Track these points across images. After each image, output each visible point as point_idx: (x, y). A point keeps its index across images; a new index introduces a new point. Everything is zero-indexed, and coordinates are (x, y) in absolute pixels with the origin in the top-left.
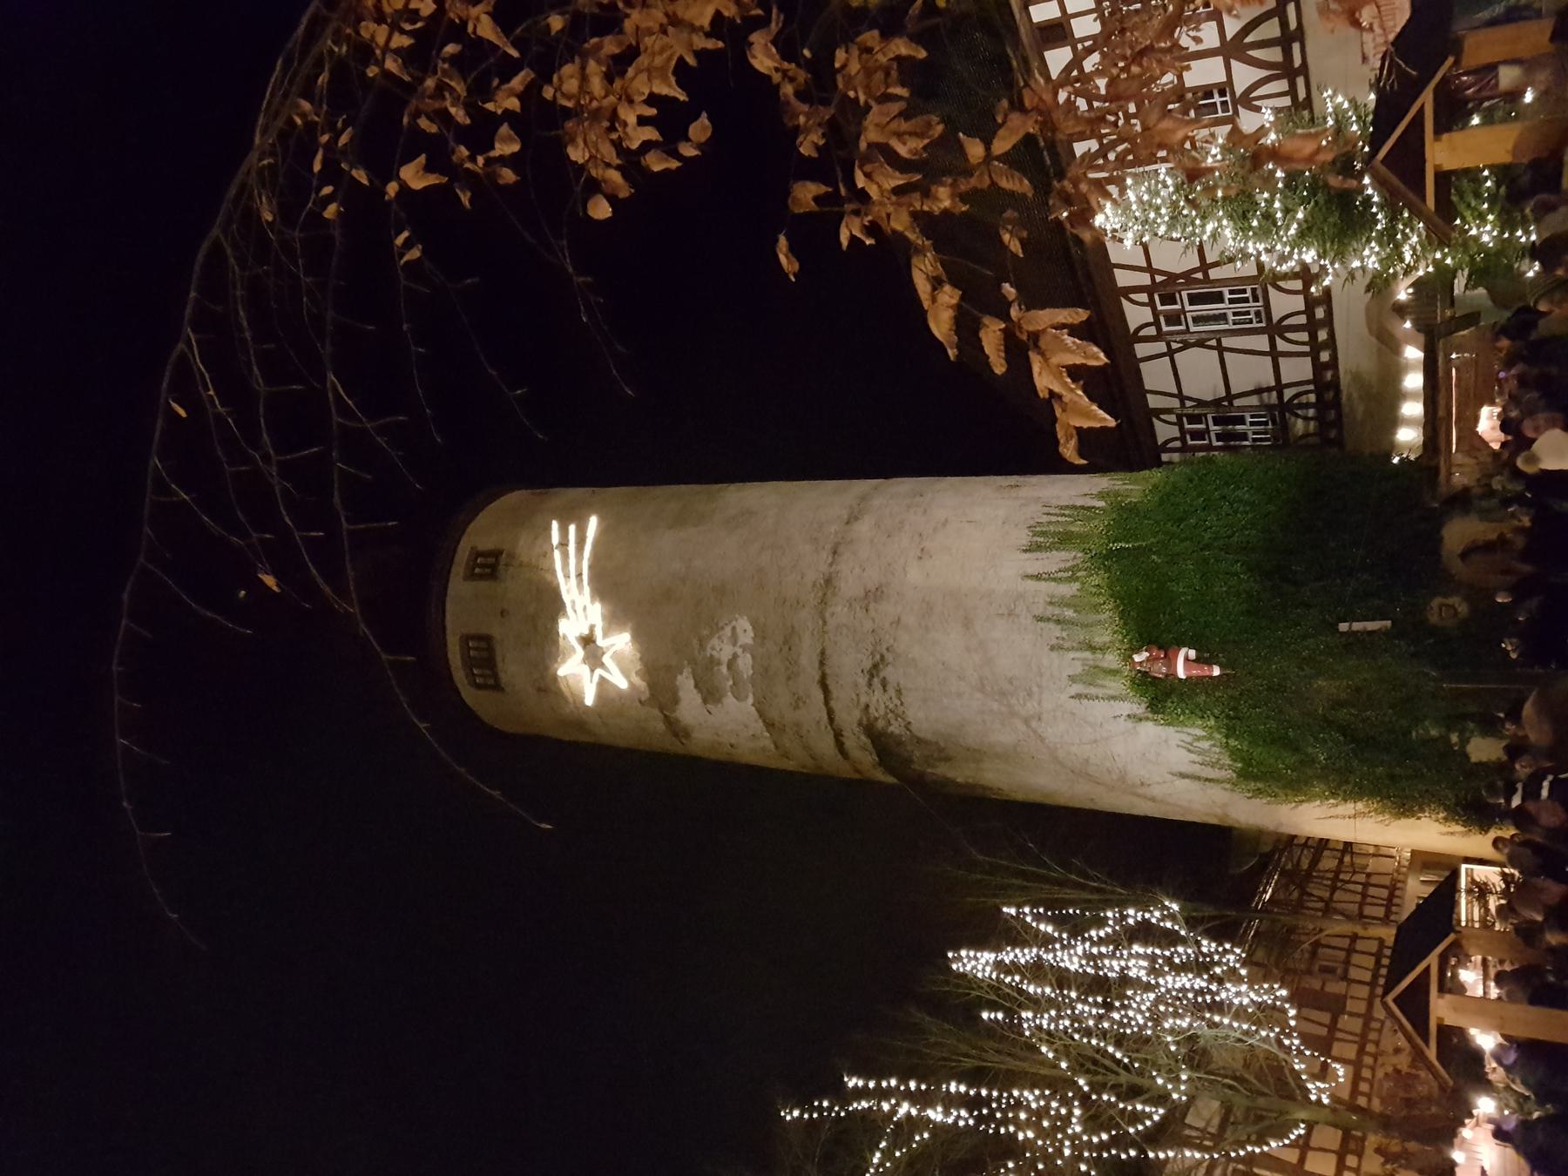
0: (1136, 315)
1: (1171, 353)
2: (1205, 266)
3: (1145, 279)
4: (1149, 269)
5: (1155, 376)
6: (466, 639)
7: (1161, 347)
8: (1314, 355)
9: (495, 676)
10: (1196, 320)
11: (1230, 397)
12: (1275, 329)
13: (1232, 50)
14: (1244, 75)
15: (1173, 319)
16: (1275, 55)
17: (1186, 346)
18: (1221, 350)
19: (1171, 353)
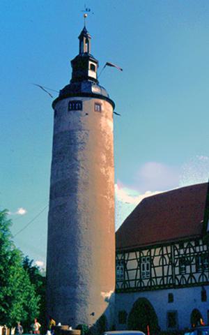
0: (145, 253)
1: (137, 259)
2: (154, 267)
3: (152, 255)
4: (154, 256)
5: (132, 256)
6: (80, 102)
7: (138, 257)
8: (135, 288)
9: (72, 109)
10: (143, 265)
11: (127, 271)
12: (141, 280)
13: (191, 275)
14: (187, 276)
15: (144, 260)
16: (189, 282)
17: (138, 262)
18: (137, 269)
19: (137, 259)
